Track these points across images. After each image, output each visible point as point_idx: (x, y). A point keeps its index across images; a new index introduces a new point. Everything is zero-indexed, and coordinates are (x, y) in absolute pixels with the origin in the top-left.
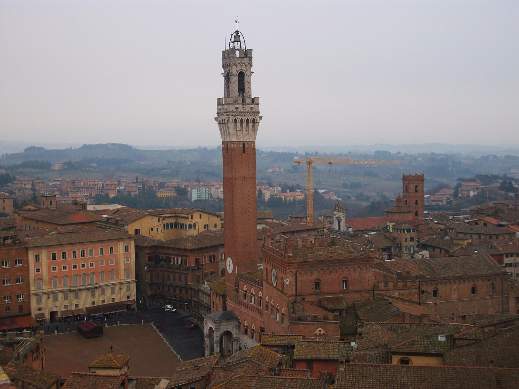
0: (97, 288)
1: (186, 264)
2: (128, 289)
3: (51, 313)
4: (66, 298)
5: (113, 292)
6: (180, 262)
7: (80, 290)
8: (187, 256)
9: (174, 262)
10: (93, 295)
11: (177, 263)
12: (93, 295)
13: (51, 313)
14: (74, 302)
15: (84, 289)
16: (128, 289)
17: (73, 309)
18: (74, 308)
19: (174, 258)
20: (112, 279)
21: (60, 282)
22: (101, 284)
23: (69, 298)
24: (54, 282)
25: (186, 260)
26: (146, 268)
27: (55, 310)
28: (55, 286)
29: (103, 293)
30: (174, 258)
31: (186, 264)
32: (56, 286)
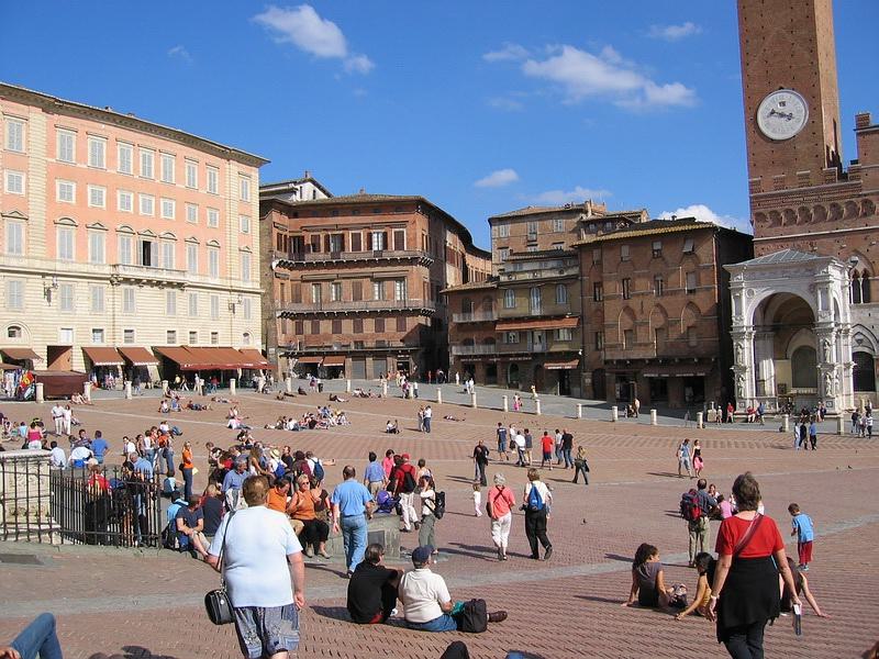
0: (180, 285)
1: (399, 246)
2: (247, 315)
3: (48, 347)
4: (98, 305)
5: (215, 317)
6: (377, 245)
7: (138, 281)
8: (403, 224)
9: (356, 247)
10: (171, 308)
11: (370, 246)
12: (171, 308)
13: (48, 347)
14: (124, 322)
15: (149, 282)
16: (247, 315)
17: (118, 345)
18: (121, 343)
19: (356, 238)
20: (213, 274)
21: (82, 245)
22: (189, 279)
23: (108, 304)
24: (62, 238)
25: (399, 236)
26: (274, 264)
27: (62, 342)
28: (66, 256)
29: (193, 311)
30: (356, 238)
31: (399, 246)
32: (70, 257)
